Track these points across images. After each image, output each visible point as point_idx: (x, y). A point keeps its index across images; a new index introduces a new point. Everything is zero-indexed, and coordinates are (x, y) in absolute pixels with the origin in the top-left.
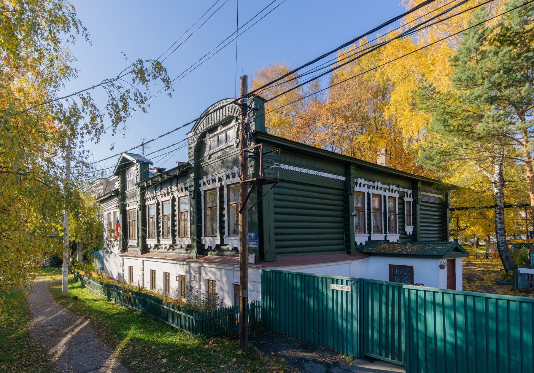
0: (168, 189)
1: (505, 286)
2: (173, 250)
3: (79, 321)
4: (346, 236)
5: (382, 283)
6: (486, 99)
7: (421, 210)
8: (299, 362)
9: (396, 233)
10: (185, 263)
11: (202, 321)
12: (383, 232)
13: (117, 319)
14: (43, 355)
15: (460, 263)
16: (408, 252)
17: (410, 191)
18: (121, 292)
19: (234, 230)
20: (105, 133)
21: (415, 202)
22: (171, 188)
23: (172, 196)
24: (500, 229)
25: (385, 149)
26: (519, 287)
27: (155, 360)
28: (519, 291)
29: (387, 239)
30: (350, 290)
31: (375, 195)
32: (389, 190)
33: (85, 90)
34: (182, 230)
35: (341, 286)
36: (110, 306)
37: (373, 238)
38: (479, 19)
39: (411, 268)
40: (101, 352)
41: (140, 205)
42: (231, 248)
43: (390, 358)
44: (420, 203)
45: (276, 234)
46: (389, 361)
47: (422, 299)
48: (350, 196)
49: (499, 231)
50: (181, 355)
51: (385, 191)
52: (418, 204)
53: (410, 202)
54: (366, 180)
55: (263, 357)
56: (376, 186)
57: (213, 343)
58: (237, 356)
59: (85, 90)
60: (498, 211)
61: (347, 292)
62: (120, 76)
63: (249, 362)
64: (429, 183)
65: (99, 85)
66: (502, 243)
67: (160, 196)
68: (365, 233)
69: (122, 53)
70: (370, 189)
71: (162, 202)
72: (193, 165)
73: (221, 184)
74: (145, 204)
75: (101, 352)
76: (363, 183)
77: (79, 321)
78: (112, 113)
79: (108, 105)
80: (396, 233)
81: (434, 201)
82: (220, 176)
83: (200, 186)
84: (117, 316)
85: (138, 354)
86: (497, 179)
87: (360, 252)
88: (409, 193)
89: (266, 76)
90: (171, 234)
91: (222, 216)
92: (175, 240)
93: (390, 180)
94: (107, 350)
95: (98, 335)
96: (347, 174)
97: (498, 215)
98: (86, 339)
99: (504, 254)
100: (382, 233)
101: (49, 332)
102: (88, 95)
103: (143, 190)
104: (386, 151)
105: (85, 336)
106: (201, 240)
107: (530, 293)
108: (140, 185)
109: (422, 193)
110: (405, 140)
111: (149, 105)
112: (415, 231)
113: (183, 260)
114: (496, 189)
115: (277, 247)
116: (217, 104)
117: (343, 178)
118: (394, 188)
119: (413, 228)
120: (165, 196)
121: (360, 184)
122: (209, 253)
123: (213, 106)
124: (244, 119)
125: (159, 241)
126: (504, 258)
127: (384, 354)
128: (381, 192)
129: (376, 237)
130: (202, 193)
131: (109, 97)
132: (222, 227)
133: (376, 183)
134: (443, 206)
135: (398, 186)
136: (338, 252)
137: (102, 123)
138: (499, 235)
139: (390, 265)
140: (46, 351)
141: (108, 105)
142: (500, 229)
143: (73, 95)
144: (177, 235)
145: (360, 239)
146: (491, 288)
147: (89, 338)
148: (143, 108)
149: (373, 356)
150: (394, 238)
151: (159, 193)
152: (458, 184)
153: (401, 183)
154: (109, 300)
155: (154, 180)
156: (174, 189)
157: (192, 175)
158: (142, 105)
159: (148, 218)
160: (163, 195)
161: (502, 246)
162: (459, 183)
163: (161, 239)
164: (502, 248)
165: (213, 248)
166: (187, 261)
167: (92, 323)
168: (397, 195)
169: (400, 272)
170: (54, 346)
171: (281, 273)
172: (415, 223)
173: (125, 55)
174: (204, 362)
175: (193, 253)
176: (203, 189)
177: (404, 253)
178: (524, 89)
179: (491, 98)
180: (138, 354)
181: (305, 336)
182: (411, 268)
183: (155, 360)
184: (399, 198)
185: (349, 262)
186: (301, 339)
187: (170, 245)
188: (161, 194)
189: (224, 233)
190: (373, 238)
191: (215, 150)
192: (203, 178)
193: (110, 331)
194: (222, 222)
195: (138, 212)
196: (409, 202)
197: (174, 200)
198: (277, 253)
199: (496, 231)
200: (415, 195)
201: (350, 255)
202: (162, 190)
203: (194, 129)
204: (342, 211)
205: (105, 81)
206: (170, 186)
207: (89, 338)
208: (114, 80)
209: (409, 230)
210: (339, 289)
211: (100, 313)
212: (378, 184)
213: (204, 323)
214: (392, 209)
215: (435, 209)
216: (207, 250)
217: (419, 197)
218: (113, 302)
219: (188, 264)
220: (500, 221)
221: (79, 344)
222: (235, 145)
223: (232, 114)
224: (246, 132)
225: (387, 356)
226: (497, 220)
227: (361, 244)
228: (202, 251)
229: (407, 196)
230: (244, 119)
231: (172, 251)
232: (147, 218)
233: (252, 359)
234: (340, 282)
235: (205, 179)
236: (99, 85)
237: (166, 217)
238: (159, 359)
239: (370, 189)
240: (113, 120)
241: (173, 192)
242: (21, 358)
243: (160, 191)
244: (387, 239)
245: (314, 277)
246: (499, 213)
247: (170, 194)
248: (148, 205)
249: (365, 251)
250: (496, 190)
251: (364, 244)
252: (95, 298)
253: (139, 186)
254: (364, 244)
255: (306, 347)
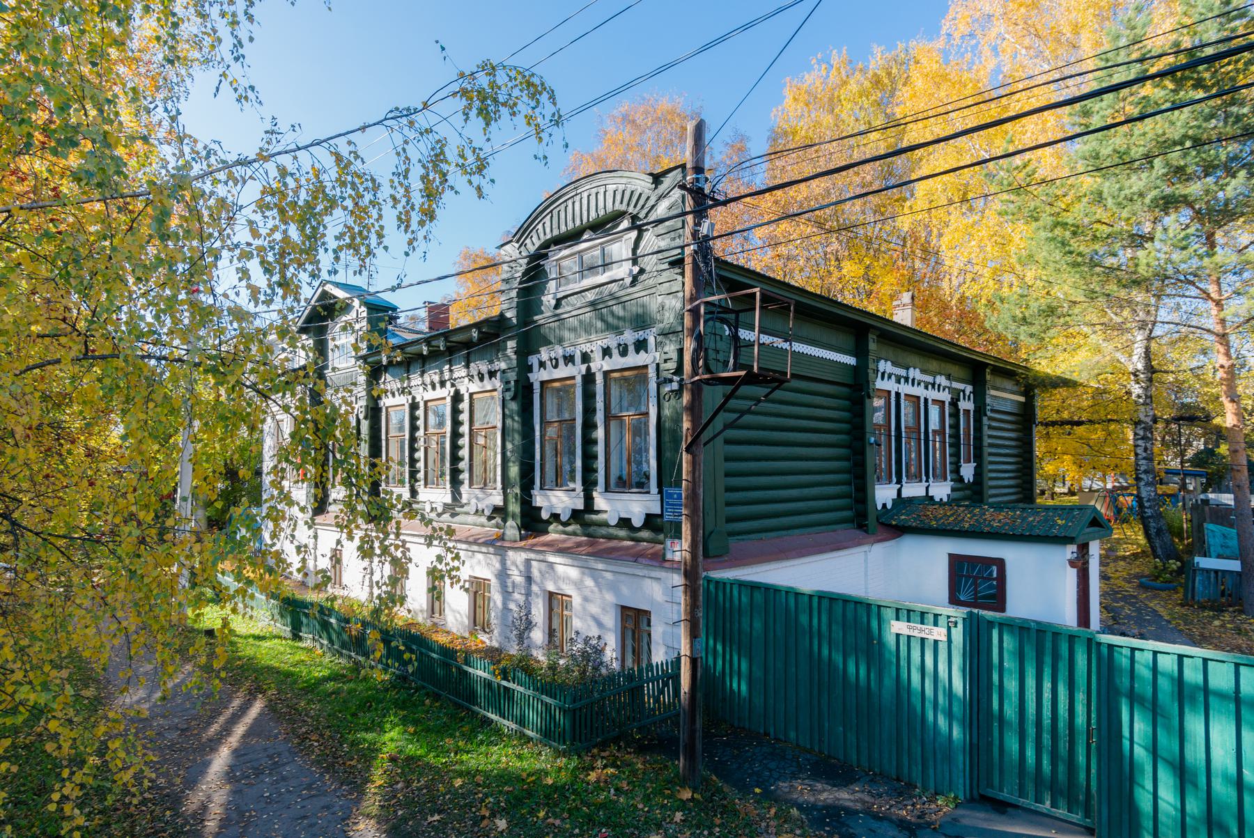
0: (442, 373)
1: (1163, 594)
2: (453, 515)
3: (236, 703)
4: (857, 490)
5: (1026, 625)
6: (1154, 200)
7: (990, 427)
8: (832, 815)
9: (945, 479)
10: (491, 550)
11: (574, 711)
12: (924, 478)
13: (333, 693)
14: (168, 813)
15: (1095, 549)
16: (992, 527)
17: (969, 389)
18: (333, 621)
19: (620, 478)
20: (386, 248)
21: (980, 410)
22: (451, 371)
23: (453, 390)
24: (1146, 472)
25: (910, 293)
26: (1197, 598)
27: (476, 824)
28: (1199, 607)
29: (930, 494)
30: (945, 639)
31: (934, 401)
32: (933, 385)
33: (344, 134)
34: (478, 470)
35: (919, 626)
36: (301, 656)
37: (905, 493)
38: (1134, 28)
39: (1000, 563)
40: (325, 800)
41: (367, 407)
42: (613, 522)
43: (1048, 803)
44: (989, 413)
45: (729, 489)
46: (1045, 811)
47: (1172, 678)
48: (867, 401)
49: (1142, 476)
50: (538, 804)
51: (898, 382)
52: (986, 415)
53: (969, 411)
54: (894, 364)
55: (747, 807)
56: (911, 377)
57: (605, 767)
58: (683, 806)
59: (344, 134)
60: (1141, 433)
61: (936, 642)
62: (429, 103)
63: (717, 821)
64: (1007, 372)
65: (378, 123)
66: (1149, 501)
67: (421, 388)
68: (890, 482)
69: (437, 42)
70: (899, 383)
71: (426, 403)
72: (514, 321)
73: (589, 369)
74: (377, 404)
75: (325, 800)
76: (888, 371)
77: (236, 703)
78: (398, 196)
79: (393, 174)
80: (945, 479)
81: (1008, 409)
82: (586, 348)
83: (530, 369)
84: (330, 686)
85: (425, 803)
86: (1140, 366)
87: (882, 524)
88: (967, 393)
89: (634, 121)
90: (448, 478)
91: (589, 442)
92: (460, 494)
93: (934, 365)
94: (335, 790)
95: (300, 744)
96: (860, 351)
97: (1140, 442)
98: (271, 757)
99: (1152, 524)
100: (921, 481)
101: (165, 738)
102: (352, 148)
103: (375, 373)
104: (913, 298)
105: (265, 750)
106: (531, 496)
107: (1223, 611)
108: (370, 360)
109: (993, 392)
110: (948, 277)
111: (493, 181)
112: (978, 473)
113: (486, 544)
114: (1137, 386)
115: (730, 520)
116: (582, 182)
117: (850, 360)
118: (941, 380)
119: (975, 468)
120: (434, 388)
121: (883, 374)
122: (551, 528)
123: (572, 186)
124: (698, 224)
125: (414, 493)
126: (1153, 531)
127: (1031, 794)
128: (919, 391)
129: (913, 490)
130: (537, 387)
131: (398, 154)
132: (589, 470)
133: (911, 370)
134: (1026, 418)
135: (949, 377)
136: (843, 526)
137: (381, 223)
138: (1142, 483)
139: (950, 555)
140: (175, 801)
141: (393, 174)
142: (1146, 472)
143: (312, 145)
144: (467, 482)
145: (884, 494)
146: (1135, 597)
147: (279, 755)
148: (479, 189)
149: (1005, 795)
150: (941, 491)
151: (416, 380)
152: (1075, 377)
153: (955, 370)
154: (296, 637)
155: (409, 349)
156: (460, 372)
157: (511, 344)
158: (476, 179)
159: (387, 440)
160: (429, 387)
161: (1150, 507)
162: (1075, 374)
163: (420, 486)
164: (1149, 512)
165: (564, 518)
166: (497, 545)
167: (271, 707)
168: (945, 396)
169: (973, 570)
170: (191, 783)
171: (770, 591)
172: (978, 457)
173: (443, 49)
174: (603, 825)
175: (512, 529)
176: (538, 376)
177: (986, 529)
178: (1236, 185)
179: (1163, 198)
180: (425, 803)
181: (820, 741)
182: (1000, 563)
183: (476, 824)
184: (950, 403)
185: (865, 548)
186: (808, 746)
187: (445, 504)
188: (424, 383)
189: (595, 483)
190: (905, 493)
191: (576, 287)
192: (539, 352)
193: (328, 733)
194: (589, 457)
195: (358, 421)
196: (967, 412)
197: (457, 398)
198: (731, 534)
199: (1137, 474)
200: (979, 396)
201: (866, 532)
202: (426, 375)
203: (518, 236)
204: (848, 433)
205: (391, 111)
206: (447, 367)
207: (279, 755)
208: (416, 111)
209: (968, 471)
210: (916, 633)
211: (285, 678)
212: (915, 373)
213: (578, 713)
214: (937, 428)
215: (1010, 426)
216: (548, 522)
217: (988, 401)
218: (308, 643)
219: (500, 552)
220: (1144, 455)
221: (257, 776)
222: (628, 281)
223: (623, 208)
224: (705, 257)
225: (1039, 800)
226: (1139, 451)
227: (884, 505)
228: (532, 523)
229: (964, 398)
230: (698, 224)
231: (450, 519)
232: (383, 437)
233: (722, 814)
234: (919, 619)
235: (544, 354)
236: (378, 123)
237: (435, 438)
238: (485, 822)
239: (899, 383)
240: (401, 213)
241: (455, 379)
242: (108, 825)
243: (422, 375)
244: (930, 494)
245: (869, 605)
246: (1142, 438)
247: (448, 384)
248: (387, 408)
249: (894, 523)
250: (1137, 390)
251: (889, 506)
252: (257, 632)
253: (365, 362)
254: (889, 506)
255: (839, 774)
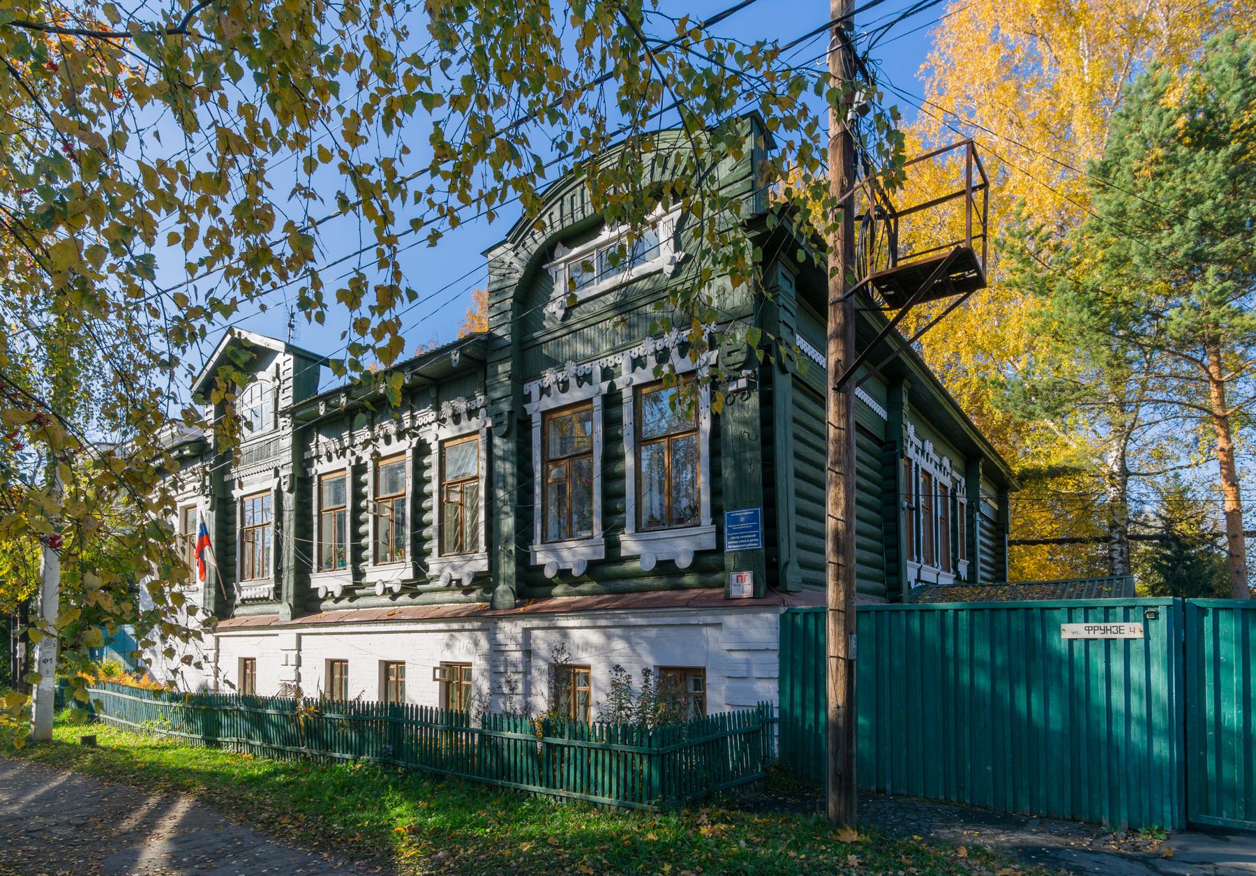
22: (413, 418)
34: (449, 536)
41: (292, 476)
73: (612, 386)
74: (306, 473)
83: (527, 399)
90: (408, 549)
122: (558, 590)
130: (536, 419)
144: (435, 551)
176: (538, 406)
197: (421, 450)
210: (1098, 635)
231: (410, 600)
232: (315, 512)
235: (549, 377)
241: (419, 427)
248: (320, 476)
